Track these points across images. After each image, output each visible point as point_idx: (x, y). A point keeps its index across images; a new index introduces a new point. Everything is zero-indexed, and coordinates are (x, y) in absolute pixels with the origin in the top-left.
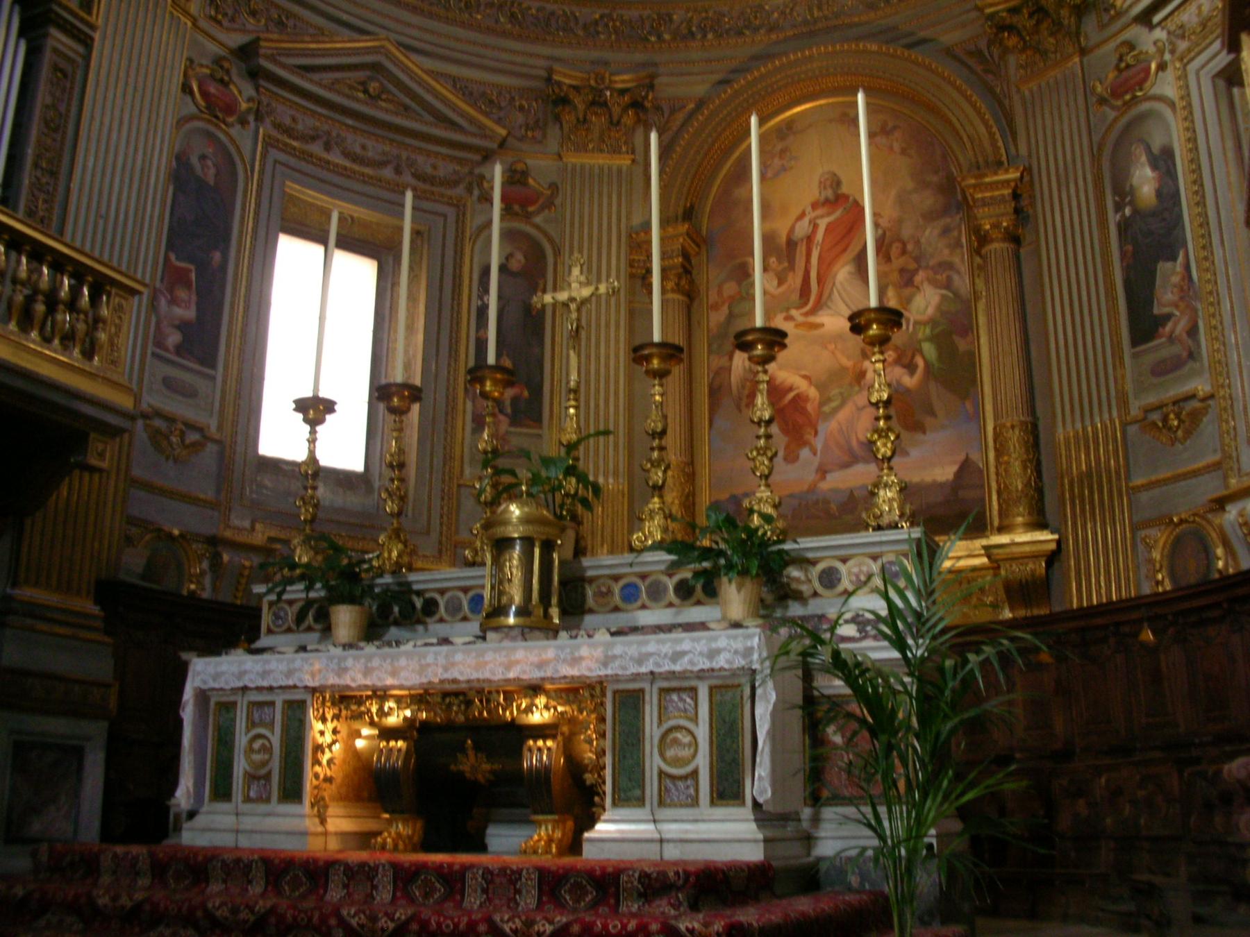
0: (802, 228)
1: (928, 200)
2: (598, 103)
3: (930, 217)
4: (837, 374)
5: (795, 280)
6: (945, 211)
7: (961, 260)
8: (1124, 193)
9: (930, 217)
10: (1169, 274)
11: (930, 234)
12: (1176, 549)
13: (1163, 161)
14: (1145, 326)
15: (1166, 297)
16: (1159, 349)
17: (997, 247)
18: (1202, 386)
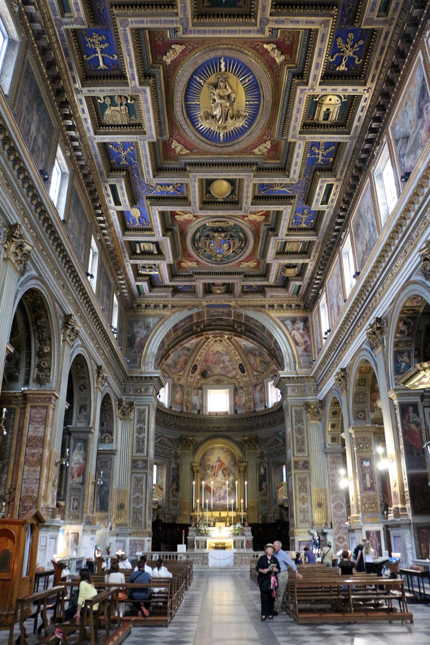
0: (214, 465)
1: (232, 463)
2: (187, 442)
3: (232, 466)
4: (218, 487)
5: (213, 472)
6: (234, 465)
7: (237, 473)
8: (260, 471)
9: (232, 466)
10: (264, 484)
11: (232, 468)
12: (262, 518)
13: (265, 469)
14: (261, 489)
15: (264, 486)
16: (262, 492)
17: (242, 473)
18: (267, 499)
